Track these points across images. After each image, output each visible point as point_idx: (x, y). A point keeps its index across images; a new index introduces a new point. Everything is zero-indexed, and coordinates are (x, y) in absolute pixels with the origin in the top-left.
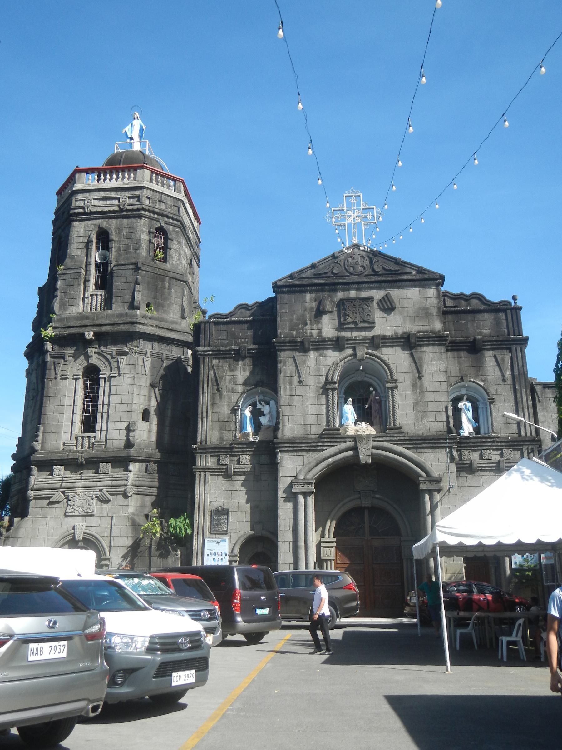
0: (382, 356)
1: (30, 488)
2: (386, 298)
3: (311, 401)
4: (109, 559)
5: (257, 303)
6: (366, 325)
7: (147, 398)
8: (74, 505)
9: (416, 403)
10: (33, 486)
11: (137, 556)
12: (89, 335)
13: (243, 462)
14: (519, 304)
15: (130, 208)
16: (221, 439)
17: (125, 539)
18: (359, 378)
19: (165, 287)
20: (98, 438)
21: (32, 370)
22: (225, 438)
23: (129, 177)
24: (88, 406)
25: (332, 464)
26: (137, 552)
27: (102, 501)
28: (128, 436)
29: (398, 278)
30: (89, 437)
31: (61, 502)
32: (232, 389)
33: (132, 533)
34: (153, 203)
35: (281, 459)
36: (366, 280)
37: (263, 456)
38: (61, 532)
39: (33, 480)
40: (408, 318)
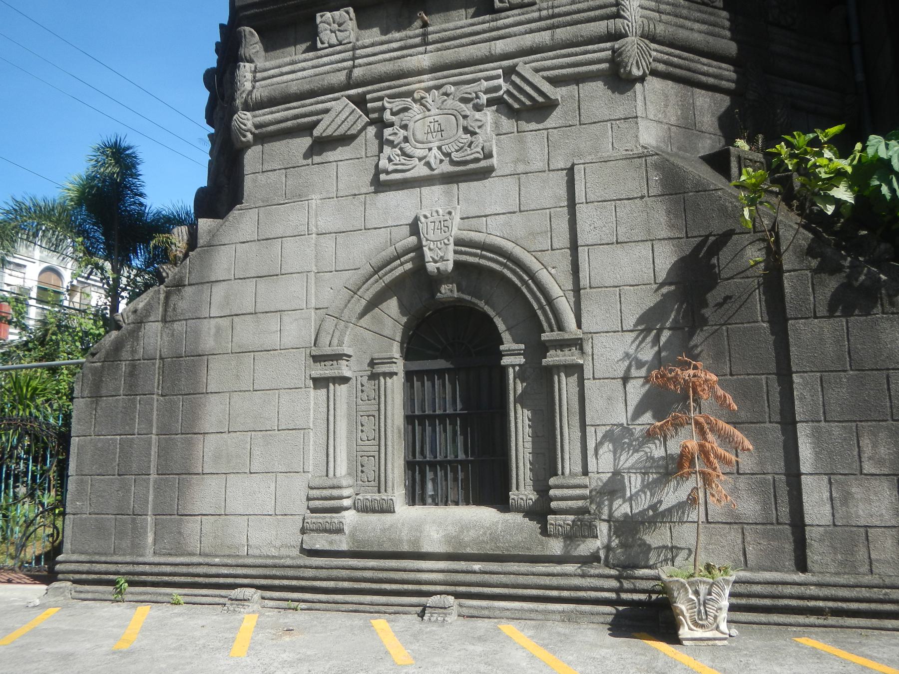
1: (239, 102)
4: (577, 344)
8: (406, 140)
10: (250, 92)
11: (704, 321)
17: (644, 250)
26: (705, 304)
27: (513, 113)
31: (353, 137)
33: (672, 226)
39: (249, 76)
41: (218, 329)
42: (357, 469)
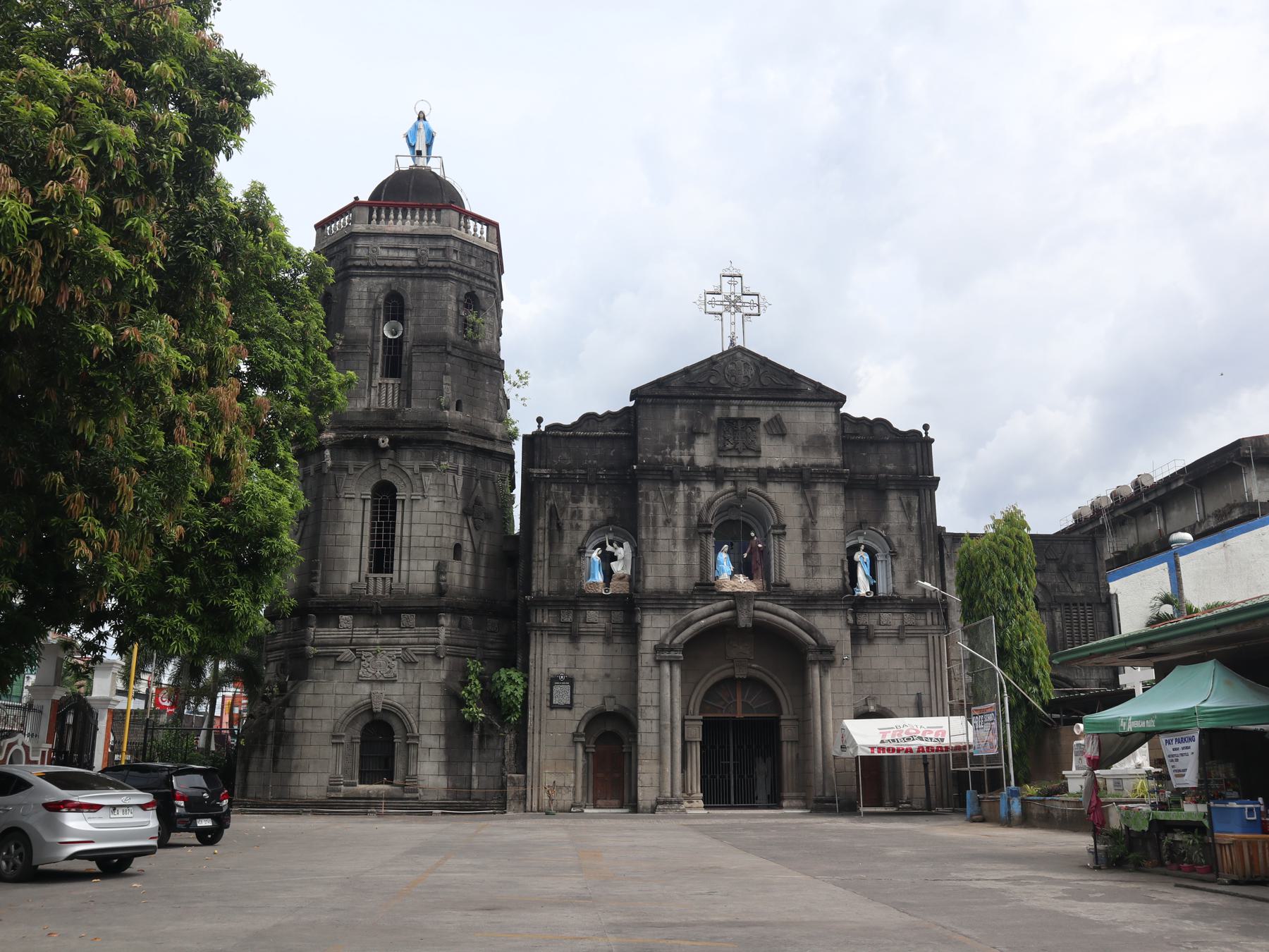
0: (769, 494)
4: (418, 737)
6: (750, 454)
9: (807, 555)
12: (384, 442)
13: (591, 620)
14: (931, 435)
15: (432, 264)
17: (438, 711)
20: (396, 580)
23: (430, 220)
24: (379, 537)
28: (438, 580)
30: (384, 579)
34: (461, 259)
35: (642, 619)
37: (617, 613)
38: (351, 701)
40: (800, 448)
42: (345, 771)
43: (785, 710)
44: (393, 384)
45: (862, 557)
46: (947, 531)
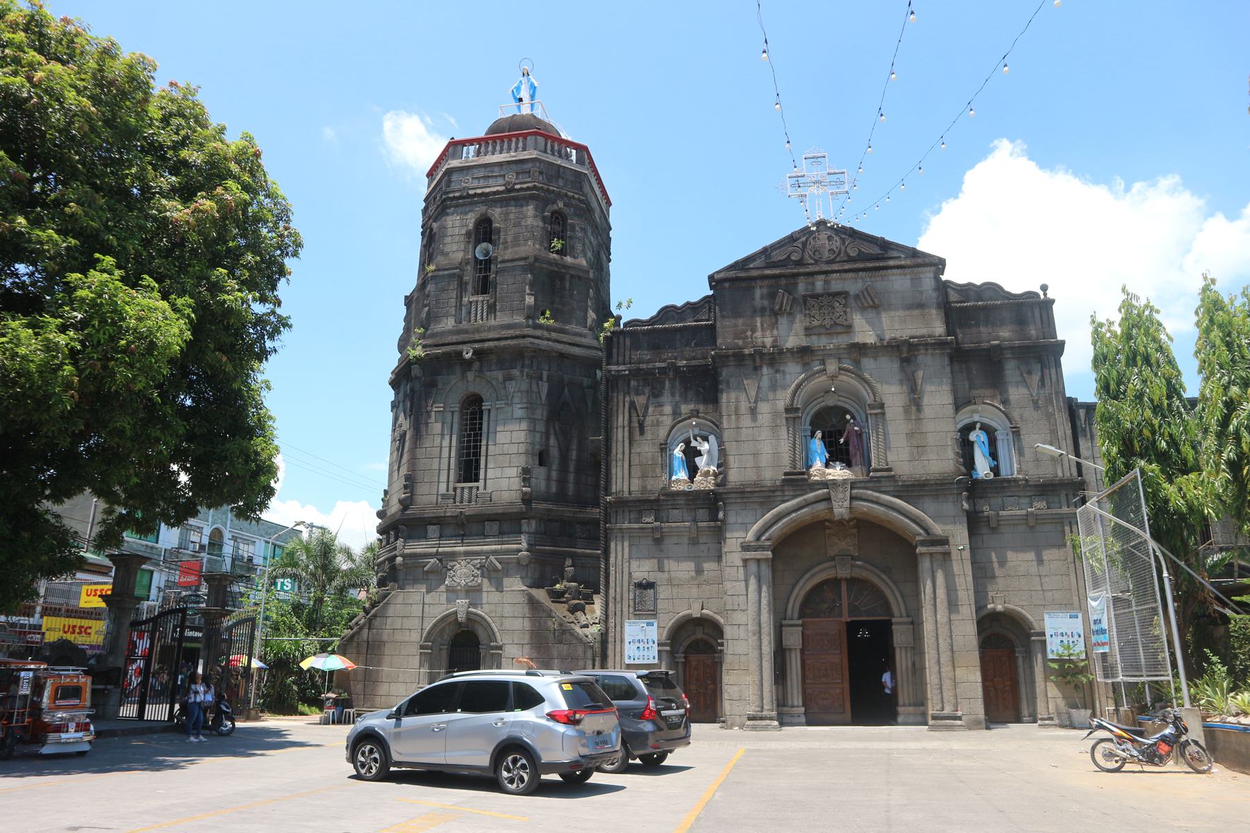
2: (865, 293)
3: (765, 434)
4: (500, 648)
5: (688, 303)
7: (544, 436)
14: (1050, 295)
15: (517, 187)
16: (644, 489)
17: (521, 620)
18: (831, 401)
19: (564, 287)
21: (399, 402)
22: (649, 487)
24: (468, 448)
25: (796, 520)
29: (881, 264)
32: (658, 420)
36: (837, 268)
41: (389, 634)
43: (896, 611)
44: (483, 301)
45: (977, 436)
46: (1079, 401)
